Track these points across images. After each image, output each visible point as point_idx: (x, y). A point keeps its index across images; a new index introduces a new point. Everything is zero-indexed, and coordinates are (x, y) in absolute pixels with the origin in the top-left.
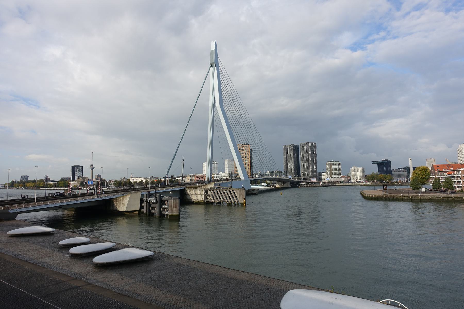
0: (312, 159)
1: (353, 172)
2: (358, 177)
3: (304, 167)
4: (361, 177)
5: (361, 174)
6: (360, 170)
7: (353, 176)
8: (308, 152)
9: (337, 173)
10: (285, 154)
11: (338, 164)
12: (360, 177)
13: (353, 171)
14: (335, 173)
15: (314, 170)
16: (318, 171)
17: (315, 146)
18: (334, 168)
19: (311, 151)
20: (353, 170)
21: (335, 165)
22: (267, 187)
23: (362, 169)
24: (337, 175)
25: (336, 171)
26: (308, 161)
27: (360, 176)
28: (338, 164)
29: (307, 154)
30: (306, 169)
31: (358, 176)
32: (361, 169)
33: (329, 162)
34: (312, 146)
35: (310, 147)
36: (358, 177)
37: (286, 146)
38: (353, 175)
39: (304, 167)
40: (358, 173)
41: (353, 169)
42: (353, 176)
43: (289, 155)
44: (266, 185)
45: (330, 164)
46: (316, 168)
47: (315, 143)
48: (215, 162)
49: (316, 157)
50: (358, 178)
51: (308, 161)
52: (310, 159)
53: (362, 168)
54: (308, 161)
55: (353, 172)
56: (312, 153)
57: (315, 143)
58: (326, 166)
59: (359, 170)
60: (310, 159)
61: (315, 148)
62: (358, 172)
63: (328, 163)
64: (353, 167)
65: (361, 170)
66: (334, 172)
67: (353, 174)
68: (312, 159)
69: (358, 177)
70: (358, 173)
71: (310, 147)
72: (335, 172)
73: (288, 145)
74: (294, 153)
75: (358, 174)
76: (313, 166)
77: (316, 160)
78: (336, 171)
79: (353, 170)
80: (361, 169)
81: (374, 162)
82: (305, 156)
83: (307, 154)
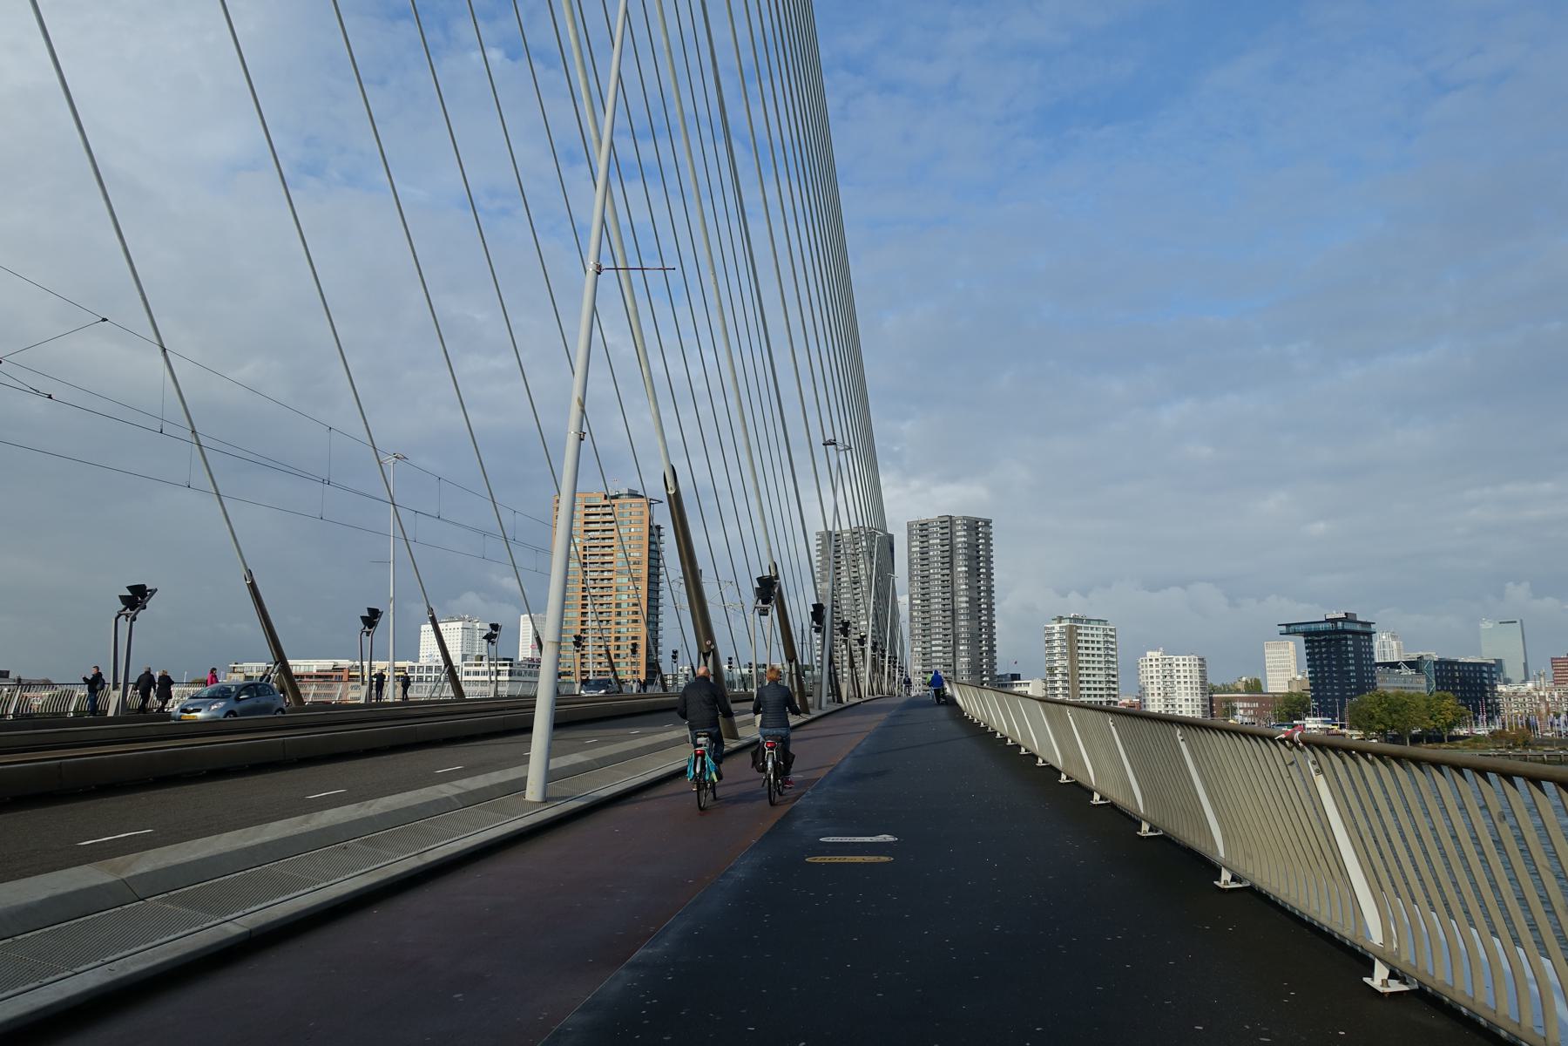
0: (974, 602)
1: (1155, 680)
2: (1184, 703)
3: (927, 645)
4: (1195, 703)
5: (1194, 691)
6: (1191, 671)
7: (1156, 697)
8: (951, 568)
9: (1100, 682)
11: (1106, 635)
12: (1193, 706)
13: (1155, 674)
14: (1091, 679)
15: (981, 660)
16: (1001, 670)
17: (988, 538)
18: (1088, 655)
19: (969, 558)
20: (1154, 669)
23: (1197, 663)
24: (1101, 689)
25: (1096, 672)
27: (1193, 700)
28: (1106, 635)
29: (946, 578)
30: (941, 648)
31: (1183, 697)
32: (1193, 663)
33: (1060, 619)
34: (973, 533)
35: (961, 538)
36: (1184, 703)
38: (1156, 692)
39: (927, 645)
40: (1182, 685)
41: (1154, 663)
42: (1156, 697)
45: (1071, 634)
46: (992, 650)
47: (987, 523)
48: (478, 625)
49: (990, 591)
51: (953, 613)
52: (964, 605)
53: (1192, 657)
54: (953, 613)
55: (1155, 680)
56: (973, 572)
57: (987, 523)
58: (1047, 642)
59: (1186, 667)
60: (962, 602)
61: (988, 544)
62: (1182, 680)
63: (1057, 627)
64: (1149, 654)
65: (1193, 668)
66: (1088, 675)
67: (1155, 686)
68: (971, 601)
69: (1180, 706)
70: (1182, 685)
72: (1094, 675)
75: (1180, 689)
76: (974, 640)
77: (990, 609)
78: (1096, 672)
79: (1154, 669)
80: (1193, 663)
81: (1288, 625)
82: (936, 589)
83: (946, 578)
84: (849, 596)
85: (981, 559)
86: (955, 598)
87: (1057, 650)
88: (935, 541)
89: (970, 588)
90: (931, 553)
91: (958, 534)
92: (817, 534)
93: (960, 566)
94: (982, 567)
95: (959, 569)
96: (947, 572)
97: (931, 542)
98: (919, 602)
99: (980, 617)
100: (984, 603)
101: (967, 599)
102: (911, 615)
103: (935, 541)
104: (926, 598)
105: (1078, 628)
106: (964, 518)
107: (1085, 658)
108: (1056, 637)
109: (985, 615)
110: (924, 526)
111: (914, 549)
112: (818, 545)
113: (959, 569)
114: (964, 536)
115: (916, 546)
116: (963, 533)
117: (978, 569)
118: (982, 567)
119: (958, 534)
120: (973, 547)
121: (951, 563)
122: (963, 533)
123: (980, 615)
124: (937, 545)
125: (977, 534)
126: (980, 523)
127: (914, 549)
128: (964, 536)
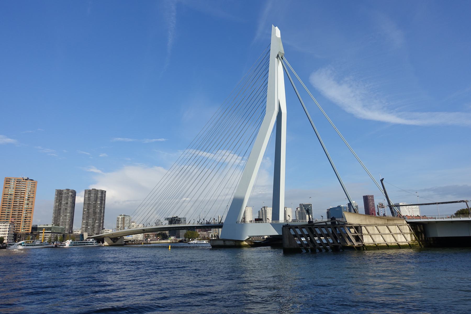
10: (58, 201)
22: (96, 244)
33: (121, 215)
34: (102, 194)
35: (99, 195)
37: (60, 190)
43: (63, 203)
44: (95, 242)
47: (105, 191)
49: (104, 208)
50: (140, 236)
57: (105, 191)
61: (105, 197)
63: (120, 217)
71: (99, 195)
73: (63, 188)
74: (72, 200)
77: (104, 212)
84: (64, 207)
85: (103, 200)
87: (120, 222)
88: (92, 195)
90: (91, 198)
91: (99, 194)
92: (56, 190)
93: (99, 202)
94: (103, 202)
95: (98, 202)
96: (95, 203)
97: (91, 195)
98: (86, 210)
100: (103, 211)
102: (83, 213)
103: (92, 195)
104: (88, 209)
105: (125, 217)
106: (101, 190)
108: (120, 219)
110: (90, 191)
111: (86, 197)
112: (56, 193)
113: (98, 202)
114: (100, 194)
115: (87, 196)
116: (100, 194)
118: (103, 202)
119: (99, 194)
120: (102, 197)
121: (96, 201)
122: (100, 194)
124: (93, 196)
127: (86, 197)
128: (100, 194)
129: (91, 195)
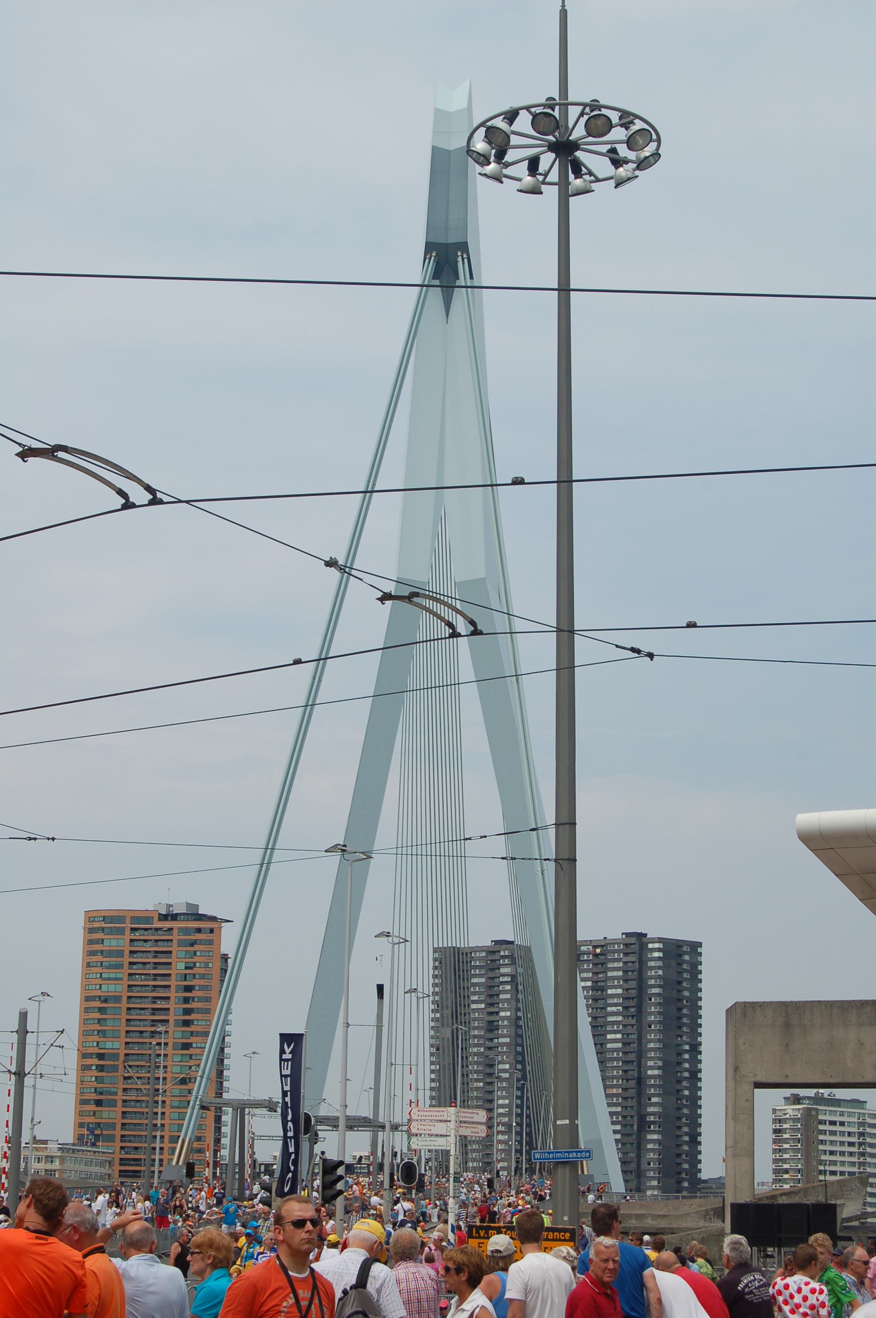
0: (670, 1067)
21: (842, 1124)
26: (641, 1081)
34: (673, 963)
47: (695, 947)
57: (695, 947)
86: (643, 1061)
88: (615, 974)
89: (666, 1046)
97: (610, 974)
99: (678, 1091)
101: (660, 1063)
103: (615, 974)
107: (828, 1148)
109: (686, 1088)
117: (679, 1018)
123: (678, 1087)
125: (680, 964)
126: (685, 949)
129: (610, 974)
